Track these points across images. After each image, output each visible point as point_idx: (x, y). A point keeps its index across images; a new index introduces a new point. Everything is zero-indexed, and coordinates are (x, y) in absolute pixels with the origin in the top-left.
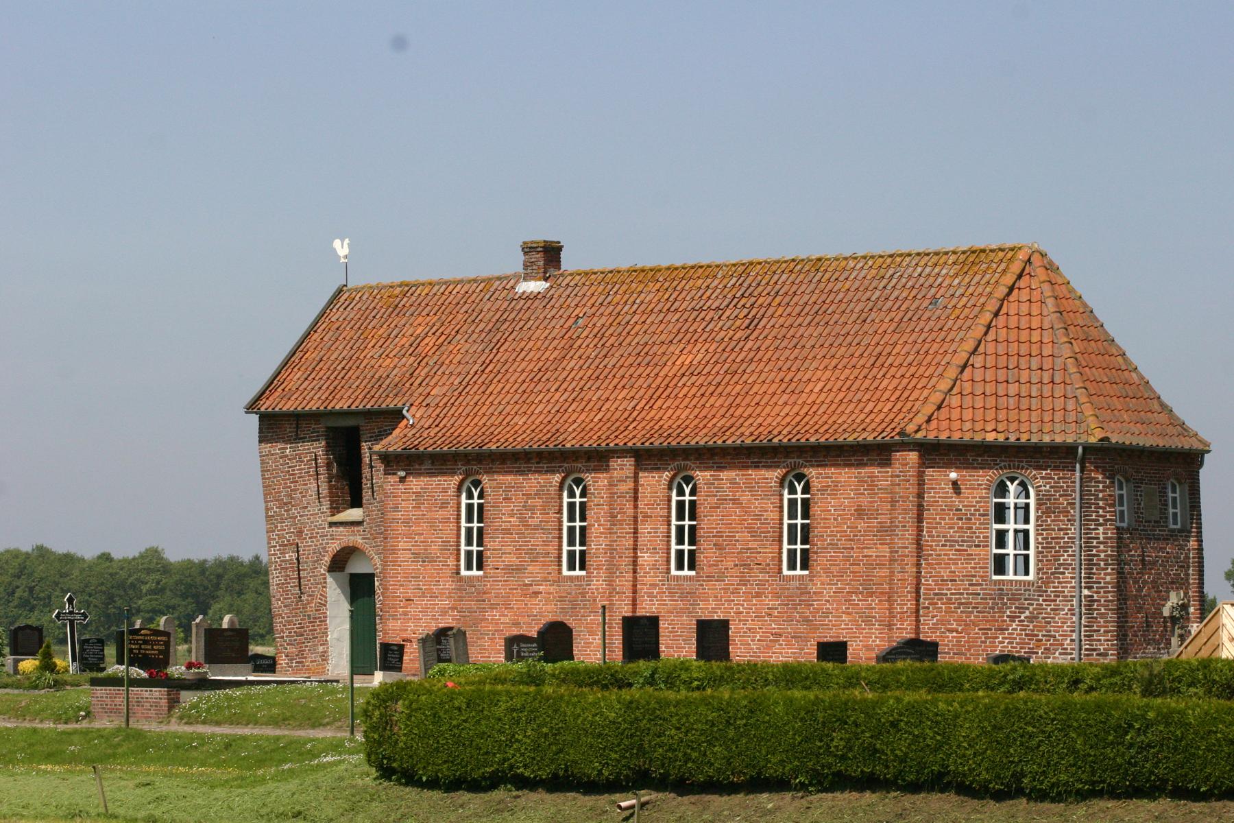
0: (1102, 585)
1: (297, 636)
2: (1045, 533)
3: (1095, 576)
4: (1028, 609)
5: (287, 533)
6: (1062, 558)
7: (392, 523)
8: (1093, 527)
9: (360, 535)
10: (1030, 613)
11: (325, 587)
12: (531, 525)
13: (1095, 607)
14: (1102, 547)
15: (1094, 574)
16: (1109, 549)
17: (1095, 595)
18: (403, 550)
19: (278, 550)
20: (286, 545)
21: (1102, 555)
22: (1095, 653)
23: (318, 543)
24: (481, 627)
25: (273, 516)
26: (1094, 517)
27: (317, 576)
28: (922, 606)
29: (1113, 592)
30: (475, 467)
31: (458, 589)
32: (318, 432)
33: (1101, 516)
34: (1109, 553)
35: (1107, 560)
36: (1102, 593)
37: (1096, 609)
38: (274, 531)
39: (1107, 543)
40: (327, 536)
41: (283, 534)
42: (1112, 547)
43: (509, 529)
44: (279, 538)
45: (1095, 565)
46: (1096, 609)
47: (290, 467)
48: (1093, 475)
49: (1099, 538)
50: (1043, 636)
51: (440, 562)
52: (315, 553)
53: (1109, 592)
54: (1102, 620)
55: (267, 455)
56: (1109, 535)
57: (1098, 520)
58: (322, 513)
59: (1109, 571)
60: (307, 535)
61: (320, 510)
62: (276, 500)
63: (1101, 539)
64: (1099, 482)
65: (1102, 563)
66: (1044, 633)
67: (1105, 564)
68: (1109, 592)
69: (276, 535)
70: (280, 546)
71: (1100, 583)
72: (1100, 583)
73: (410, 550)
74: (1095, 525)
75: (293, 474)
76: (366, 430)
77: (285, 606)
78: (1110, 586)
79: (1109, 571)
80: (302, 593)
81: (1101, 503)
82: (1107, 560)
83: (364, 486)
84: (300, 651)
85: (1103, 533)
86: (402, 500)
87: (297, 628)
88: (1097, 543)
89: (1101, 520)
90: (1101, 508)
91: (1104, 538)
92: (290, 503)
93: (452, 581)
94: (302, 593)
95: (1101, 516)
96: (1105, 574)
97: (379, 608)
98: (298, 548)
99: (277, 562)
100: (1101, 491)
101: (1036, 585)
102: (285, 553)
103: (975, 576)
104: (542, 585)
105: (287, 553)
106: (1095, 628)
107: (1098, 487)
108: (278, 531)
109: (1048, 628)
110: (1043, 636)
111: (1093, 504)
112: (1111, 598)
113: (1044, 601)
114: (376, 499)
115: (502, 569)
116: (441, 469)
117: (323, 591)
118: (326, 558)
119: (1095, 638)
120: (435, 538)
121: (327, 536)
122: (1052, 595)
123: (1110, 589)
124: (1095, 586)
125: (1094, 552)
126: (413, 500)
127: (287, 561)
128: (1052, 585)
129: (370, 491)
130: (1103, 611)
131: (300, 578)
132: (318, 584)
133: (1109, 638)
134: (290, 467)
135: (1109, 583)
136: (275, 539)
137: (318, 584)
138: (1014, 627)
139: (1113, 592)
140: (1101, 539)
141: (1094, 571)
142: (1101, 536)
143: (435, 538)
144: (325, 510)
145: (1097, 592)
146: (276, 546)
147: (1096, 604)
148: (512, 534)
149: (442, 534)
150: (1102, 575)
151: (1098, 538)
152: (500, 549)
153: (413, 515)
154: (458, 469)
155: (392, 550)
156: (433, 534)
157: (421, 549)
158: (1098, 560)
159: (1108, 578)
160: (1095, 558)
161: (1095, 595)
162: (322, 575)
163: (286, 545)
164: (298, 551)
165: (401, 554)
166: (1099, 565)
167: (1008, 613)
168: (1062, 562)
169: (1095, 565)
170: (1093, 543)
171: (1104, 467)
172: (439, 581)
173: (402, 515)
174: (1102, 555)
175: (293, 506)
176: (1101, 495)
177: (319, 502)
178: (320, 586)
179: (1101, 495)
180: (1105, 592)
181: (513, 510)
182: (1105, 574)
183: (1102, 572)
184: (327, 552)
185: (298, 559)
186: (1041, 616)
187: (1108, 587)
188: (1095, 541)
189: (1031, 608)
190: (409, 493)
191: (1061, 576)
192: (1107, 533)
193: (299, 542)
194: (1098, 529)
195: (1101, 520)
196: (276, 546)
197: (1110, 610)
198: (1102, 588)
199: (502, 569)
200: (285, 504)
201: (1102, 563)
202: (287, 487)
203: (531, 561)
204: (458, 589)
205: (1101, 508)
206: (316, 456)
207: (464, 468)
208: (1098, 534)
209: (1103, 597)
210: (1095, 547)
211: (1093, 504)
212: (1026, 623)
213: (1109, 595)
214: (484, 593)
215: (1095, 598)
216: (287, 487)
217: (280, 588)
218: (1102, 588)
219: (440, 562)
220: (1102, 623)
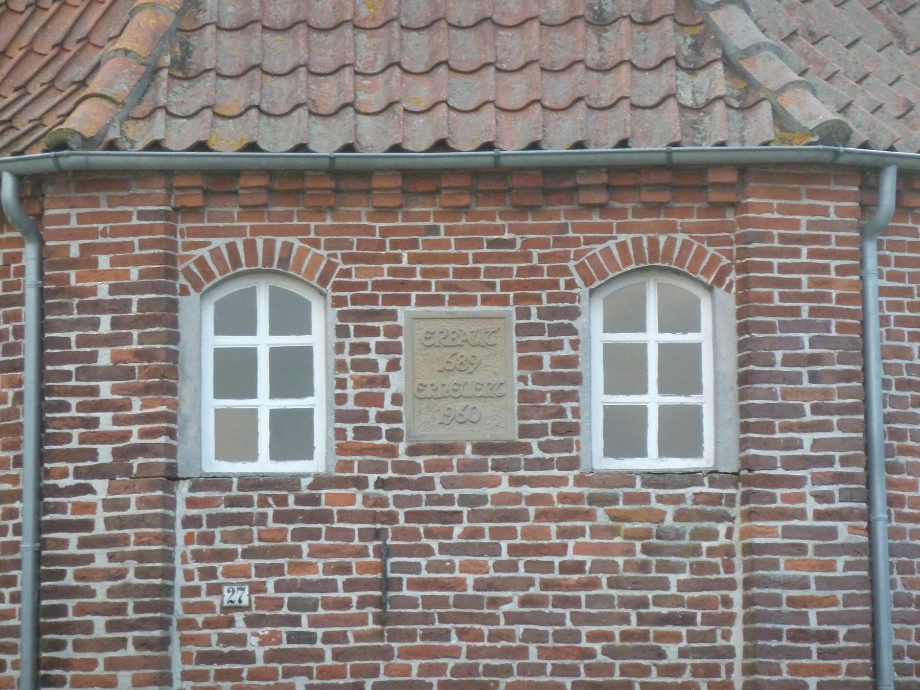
8: (70, 481)
14: (101, 558)
15: (65, 664)
16: (132, 565)
21: (101, 589)
26: (74, 444)
33: (106, 438)
34: (131, 578)
35: (121, 609)
39: (125, 540)
42: (139, 556)
48: (73, 282)
49: (88, 525)
56: (133, 510)
57: (93, 455)
59: (130, 651)
63: (100, 529)
64: (99, 307)
65: (99, 622)
67: (111, 627)
74: (78, 473)
81: (106, 390)
82: (121, 609)
85: (109, 505)
88: (83, 543)
89: (105, 453)
90: (104, 406)
91: (109, 523)
95: (106, 438)
96: (111, 664)
100: (106, 341)
107: (95, 324)
111: (73, 392)
125: (69, 580)
140: (100, 529)
141: (68, 653)
142: (99, 517)
158: (80, 610)
160: (71, 603)
166: (88, 628)
170: (64, 543)
171: (121, 247)
174: (101, 589)
176: (105, 357)
179: (105, 357)
182: (111, 664)
183: (101, 657)
188: (73, 538)
192: (125, 505)
194: (90, 490)
195: (105, 453)
201: (99, 622)
205: (104, 406)
208: (90, 508)
210: (73, 560)
211: (73, 392)
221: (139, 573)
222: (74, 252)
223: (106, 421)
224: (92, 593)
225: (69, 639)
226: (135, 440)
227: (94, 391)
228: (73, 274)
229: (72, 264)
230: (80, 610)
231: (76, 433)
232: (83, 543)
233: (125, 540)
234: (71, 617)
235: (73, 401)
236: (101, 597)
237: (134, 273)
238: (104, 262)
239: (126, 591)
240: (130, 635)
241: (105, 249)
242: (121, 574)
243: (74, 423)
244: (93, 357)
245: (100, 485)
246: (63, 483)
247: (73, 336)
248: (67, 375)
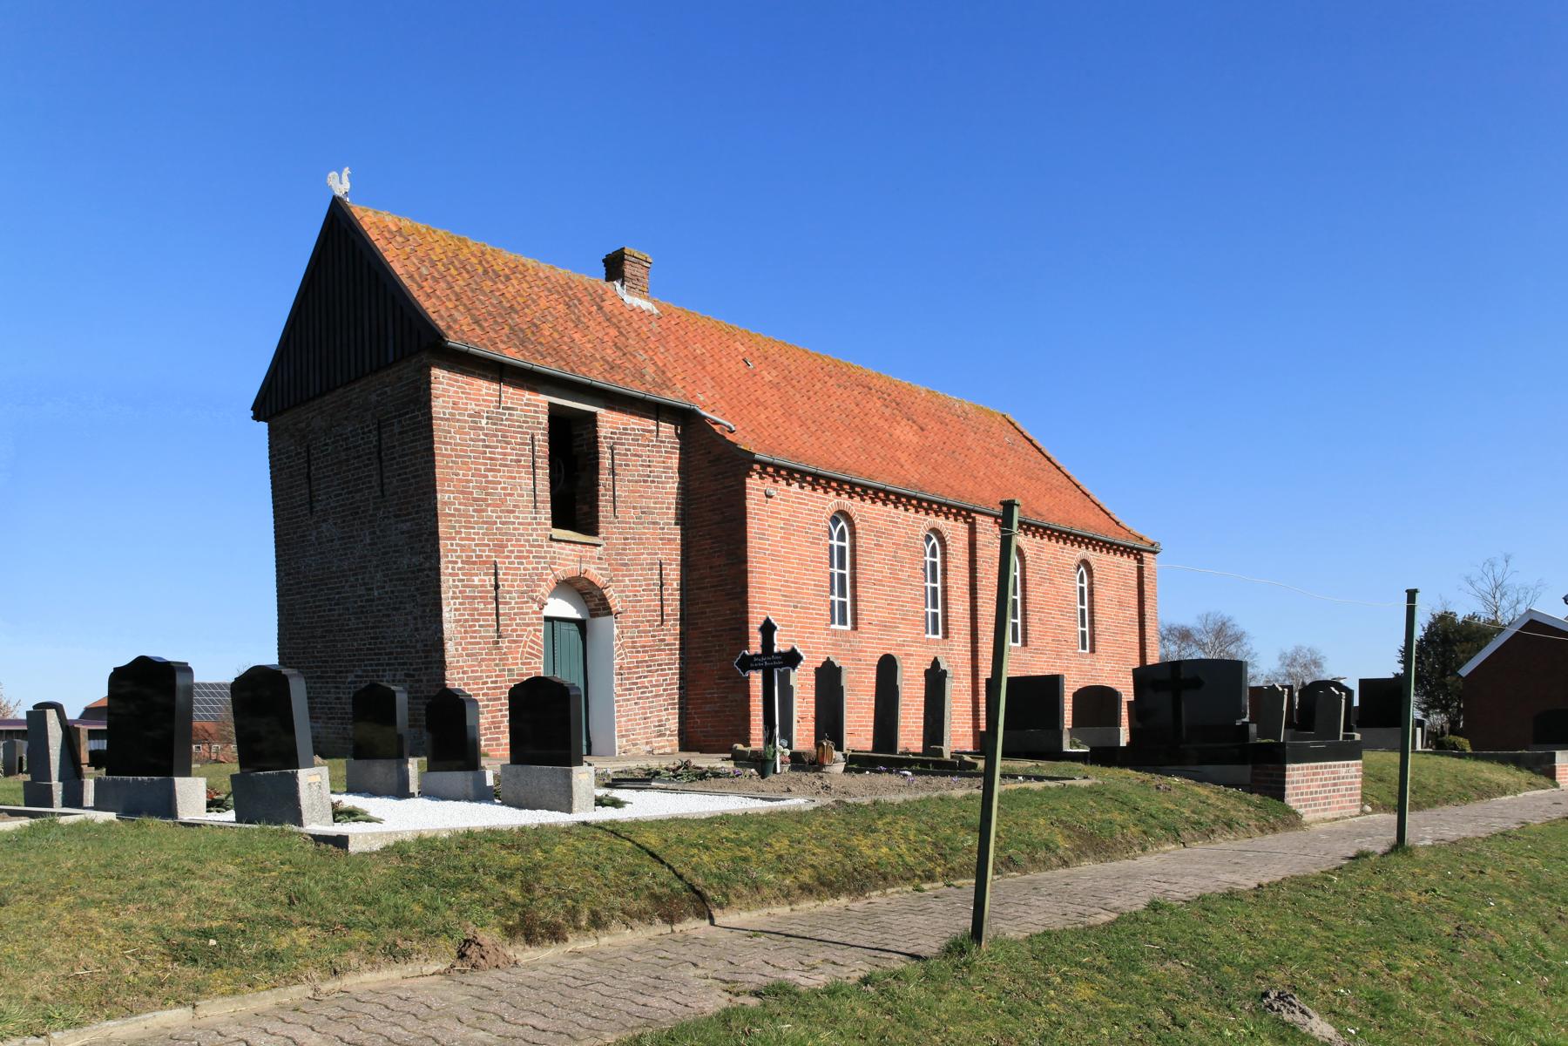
1: (488, 700)
5: (476, 545)
7: (759, 553)
9: (594, 563)
11: (540, 631)
12: (900, 579)
18: (771, 589)
19: (459, 569)
20: (474, 563)
23: (530, 566)
24: (859, 691)
25: (453, 515)
27: (527, 614)
30: (846, 502)
31: (833, 645)
32: (538, 406)
38: (454, 539)
40: (545, 557)
41: (470, 546)
43: (881, 580)
44: (462, 551)
47: (487, 447)
51: (813, 609)
52: (525, 580)
55: (447, 420)
58: (539, 524)
60: (512, 552)
61: (535, 518)
62: (462, 492)
69: (457, 545)
70: (463, 562)
73: (780, 590)
75: (491, 459)
76: (607, 422)
77: (467, 655)
80: (499, 637)
83: (601, 498)
84: (493, 723)
86: (769, 526)
87: (488, 688)
92: (486, 500)
93: (827, 634)
94: (499, 637)
97: (617, 664)
98: (496, 569)
99: (457, 587)
102: (472, 575)
104: (912, 646)
105: (476, 575)
108: (461, 539)
114: (617, 518)
115: (876, 625)
116: (812, 496)
117: (535, 635)
118: (542, 590)
120: (808, 579)
121: (545, 557)
126: (782, 528)
127: (476, 586)
129: (610, 507)
131: (497, 614)
132: (528, 625)
134: (487, 447)
136: (456, 551)
137: (528, 625)
143: (808, 579)
144: (543, 521)
146: (456, 562)
148: (884, 586)
149: (814, 575)
152: (873, 602)
153: (782, 547)
154: (830, 501)
155: (759, 588)
156: (805, 574)
157: (792, 592)
162: (534, 612)
163: (474, 563)
164: (496, 574)
165: (770, 594)
172: (813, 633)
173: (770, 545)
175: (489, 505)
177: (535, 507)
178: (531, 628)
181: (884, 559)
184: (545, 580)
185: (497, 587)
190: (777, 518)
193: (497, 560)
196: (456, 562)
199: (876, 625)
200: (475, 500)
202: (481, 476)
203: (903, 619)
204: (833, 645)
206: (533, 438)
207: (836, 501)
214: (861, 651)
216: (481, 476)
217: (462, 626)
219: (813, 609)
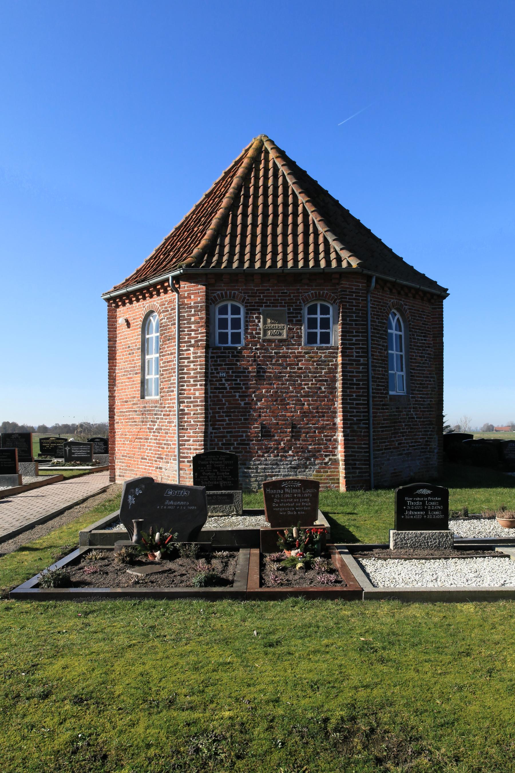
0: (192, 400)
2: (164, 358)
3: (185, 392)
4: (156, 422)
6: (172, 378)
8: (185, 348)
10: (158, 425)
13: (186, 419)
16: (199, 367)
17: (186, 409)
21: (192, 372)
22: (186, 460)
26: (186, 340)
28: (116, 421)
29: (201, 406)
33: (193, 338)
34: (199, 370)
35: (196, 377)
36: (192, 408)
37: (185, 422)
42: (200, 365)
45: (185, 382)
46: (185, 422)
48: (186, 302)
49: (189, 358)
50: (165, 444)
53: (198, 406)
54: (191, 431)
56: (199, 354)
57: (190, 342)
59: (198, 387)
63: (192, 359)
64: (191, 307)
65: (192, 380)
66: (165, 442)
67: (194, 381)
68: (198, 406)
71: (190, 398)
72: (190, 398)
78: (198, 400)
79: (198, 387)
81: (193, 327)
82: (196, 377)
85: (194, 353)
88: (188, 362)
89: (193, 341)
90: (192, 330)
91: (194, 357)
96: (194, 390)
100: (193, 315)
101: (159, 402)
103: (134, 397)
106: (185, 438)
109: (167, 438)
110: (165, 444)
112: (199, 411)
113: (164, 415)
119: (186, 446)
122: (168, 409)
123: (199, 403)
124: (186, 400)
125: (185, 371)
128: (167, 402)
130: (192, 423)
133: (198, 447)
135: (198, 398)
138: (151, 437)
139: (201, 406)
140: (192, 359)
141: (185, 387)
142: (192, 356)
145: (187, 407)
147: (186, 416)
150: (192, 391)
151: (189, 358)
158: (188, 378)
159: (197, 394)
160: (186, 376)
161: (186, 409)
166: (189, 382)
167: (148, 426)
168: (172, 382)
169: (185, 382)
170: (184, 362)
171: (196, 293)
176: (193, 319)
179: (193, 319)
180: (194, 406)
182: (194, 390)
183: (192, 388)
186: (163, 428)
187: (197, 402)
188: (186, 361)
189: (158, 421)
191: (172, 393)
194: (189, 350)
197: (199, 422)
198: (191, 402)
201: (192, 380)
205: (192, 330)
208: (189, 354)
209: (192, 410)
210: (186, 366)
211: (185, 328)
212: (156, 434)
213: (198, 408)
215: (186, 411)
218: (191, 402)
220: (192, 434)
221: (201, 369)
222: (186, 295)
223: (193, 333)
224: (190, 374)
225: (185, 384)
226: (199, 338)
227: (190, 327)
228: (186, 300)
229: (185, 298)
230: (188, 378)
231: (186, 337)
232: (188, 362)
233: (197, 361)
234: (186, 379)
235: (186, 330)
236: (192, 374)
237: (199, 299)
238: (192, 297)
239: (197, 373)
240: (198, 383)
241: (193, 294)
242: (196, 369)
243: (186, 335)
244: (190, 319)
245: (192, 349)
246: (184, 349)
247: (186, 314)
248: (185, 324)
